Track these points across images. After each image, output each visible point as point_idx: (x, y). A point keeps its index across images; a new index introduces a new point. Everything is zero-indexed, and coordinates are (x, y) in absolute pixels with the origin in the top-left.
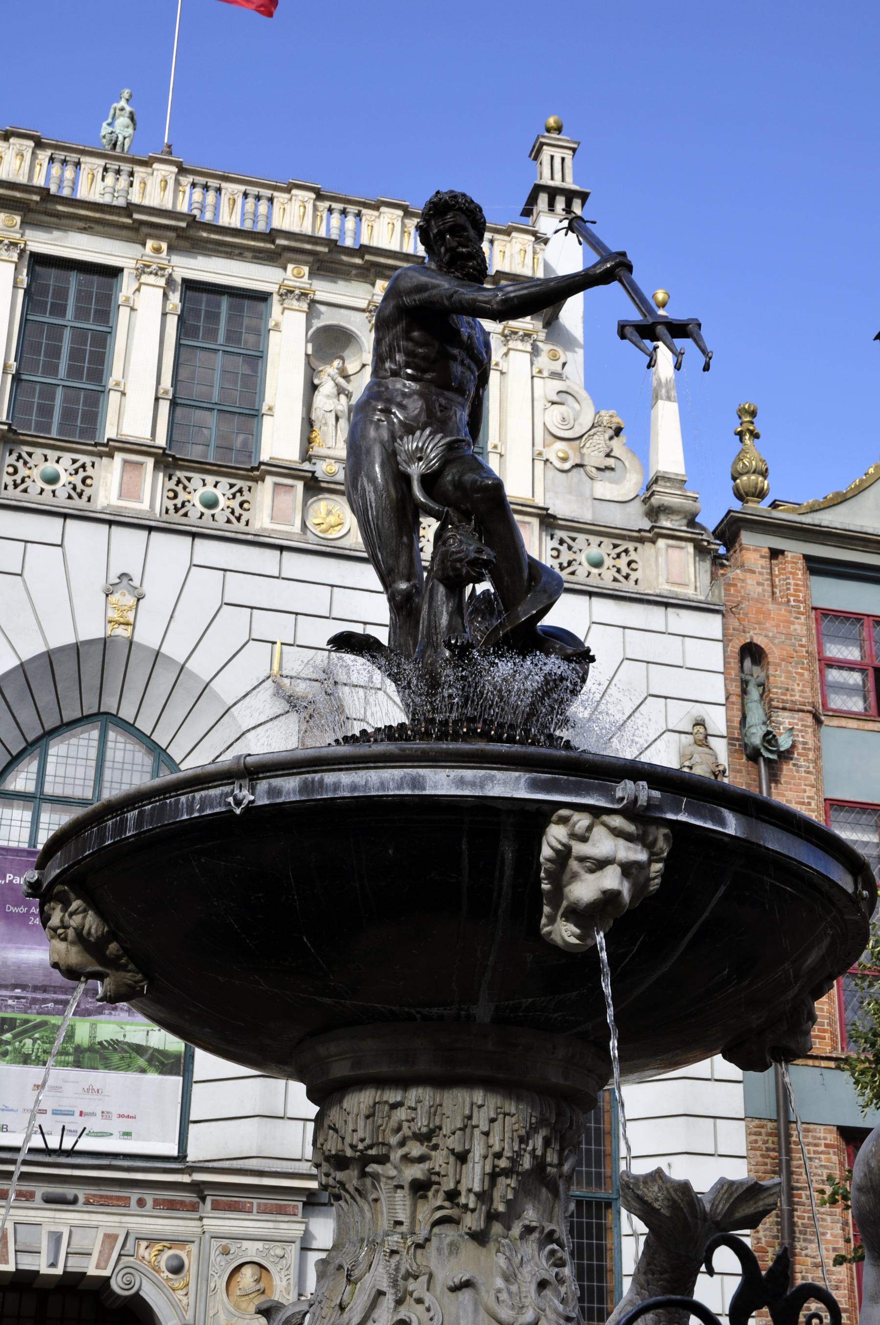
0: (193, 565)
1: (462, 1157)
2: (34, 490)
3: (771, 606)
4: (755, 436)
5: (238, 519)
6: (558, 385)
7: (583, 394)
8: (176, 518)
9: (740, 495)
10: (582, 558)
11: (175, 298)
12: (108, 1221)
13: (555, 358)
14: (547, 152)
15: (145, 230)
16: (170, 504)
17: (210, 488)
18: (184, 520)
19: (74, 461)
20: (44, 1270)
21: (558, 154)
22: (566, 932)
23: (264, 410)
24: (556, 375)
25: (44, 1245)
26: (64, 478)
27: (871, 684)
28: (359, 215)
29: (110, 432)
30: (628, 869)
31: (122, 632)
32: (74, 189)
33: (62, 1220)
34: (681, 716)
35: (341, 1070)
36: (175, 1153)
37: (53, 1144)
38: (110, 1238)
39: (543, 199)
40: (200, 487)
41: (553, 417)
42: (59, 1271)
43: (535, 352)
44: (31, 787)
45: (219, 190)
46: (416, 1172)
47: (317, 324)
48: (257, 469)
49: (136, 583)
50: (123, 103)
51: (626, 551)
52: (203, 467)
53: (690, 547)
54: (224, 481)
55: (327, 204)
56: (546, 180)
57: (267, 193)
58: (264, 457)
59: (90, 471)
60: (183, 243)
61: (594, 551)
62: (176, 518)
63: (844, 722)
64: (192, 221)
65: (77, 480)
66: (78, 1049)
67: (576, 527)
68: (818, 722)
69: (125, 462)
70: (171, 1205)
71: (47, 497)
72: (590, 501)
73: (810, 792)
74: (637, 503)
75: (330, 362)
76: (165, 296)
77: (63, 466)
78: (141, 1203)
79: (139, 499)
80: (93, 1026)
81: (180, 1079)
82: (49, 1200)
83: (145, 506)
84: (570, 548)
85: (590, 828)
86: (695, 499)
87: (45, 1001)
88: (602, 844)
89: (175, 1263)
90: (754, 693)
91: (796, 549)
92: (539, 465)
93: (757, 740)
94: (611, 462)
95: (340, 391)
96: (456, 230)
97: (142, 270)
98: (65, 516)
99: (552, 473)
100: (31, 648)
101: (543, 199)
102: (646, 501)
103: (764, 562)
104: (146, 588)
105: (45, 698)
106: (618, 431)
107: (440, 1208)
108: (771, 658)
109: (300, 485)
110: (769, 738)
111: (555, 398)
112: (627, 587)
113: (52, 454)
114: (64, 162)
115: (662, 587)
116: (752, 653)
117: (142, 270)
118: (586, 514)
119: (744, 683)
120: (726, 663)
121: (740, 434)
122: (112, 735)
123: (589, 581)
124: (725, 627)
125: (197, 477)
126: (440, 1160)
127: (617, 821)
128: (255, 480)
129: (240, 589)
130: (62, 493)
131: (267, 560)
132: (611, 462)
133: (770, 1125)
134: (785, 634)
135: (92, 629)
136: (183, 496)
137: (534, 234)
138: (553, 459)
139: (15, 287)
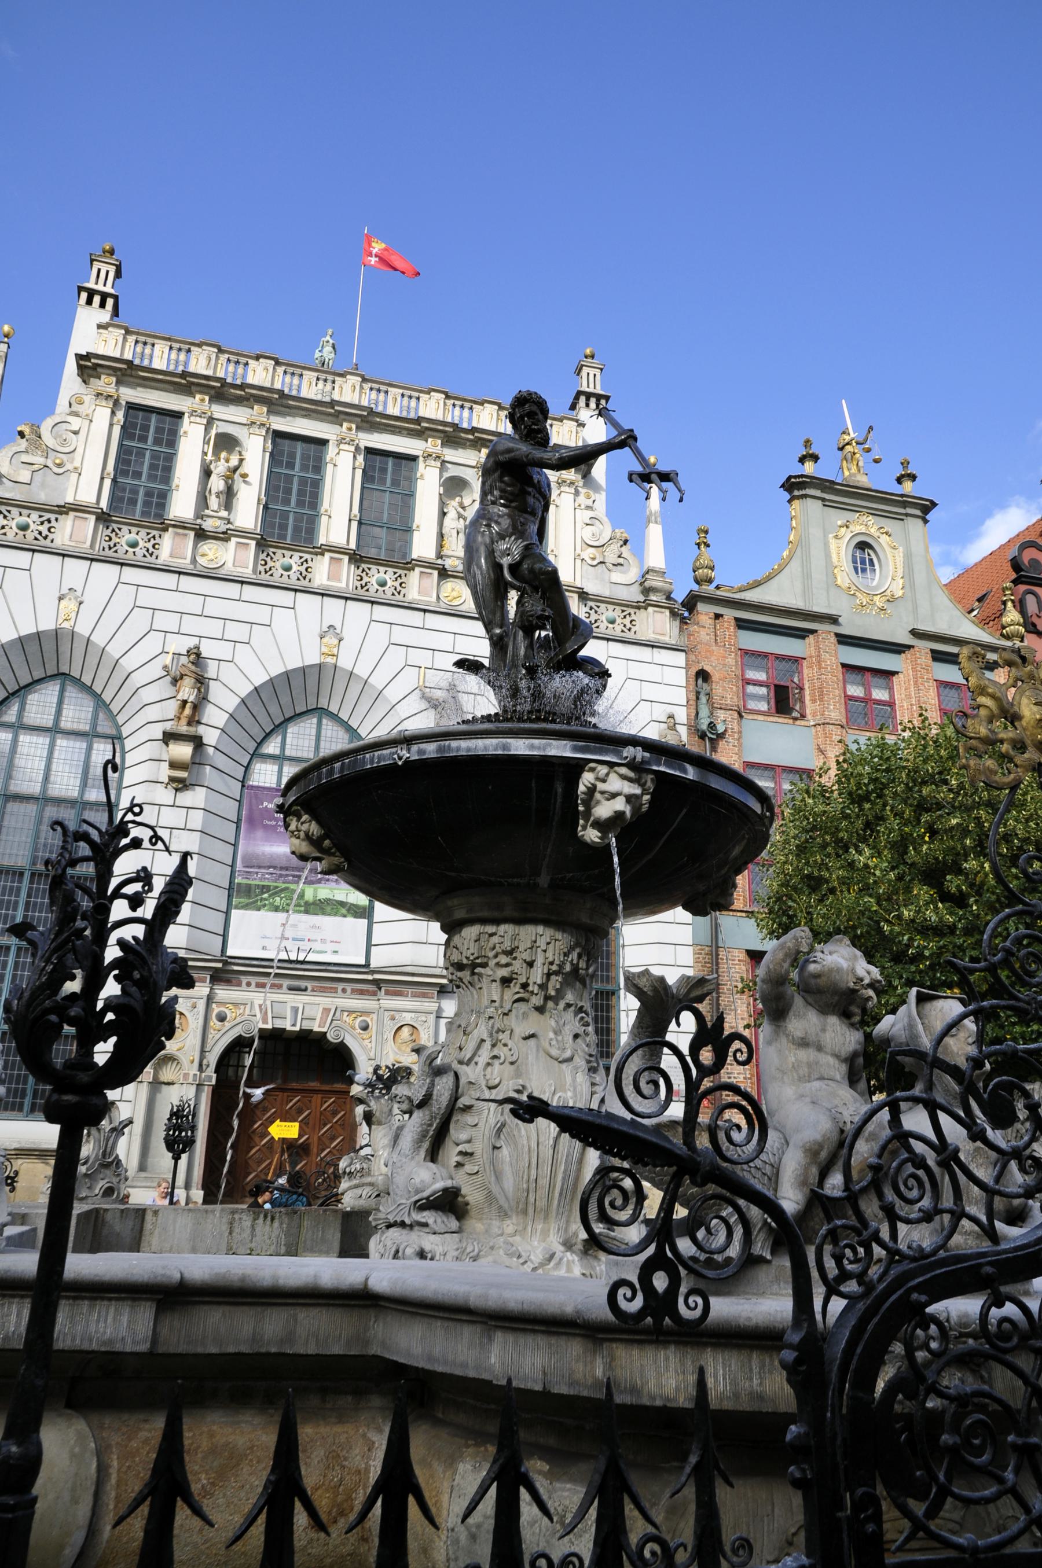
0: (372, 620)
1: (530, 964)
2: (277, 575)
3: (714, 648)
4: (707, 545)
5: (399, 593)
6: (591, 514)
7: (605, 519)
8: (362, 592)
9: (697, 581)
10: (603, 618)
11: (360, 459)
12: (325, 1001)
13: (588, 497)
14: (585, 370)
15: (342, 417)
16: (358, 584)
17: (382, 574)
18: (366, 594)
19: (301, 558)
20: (289, 1028)
21: (592, 371)
22: (592, 835)
23: (414, 527)
25: (289, 1014)
26: (295, 568)
27: (772, 694)
28: (471, 408)
29: (322, 540)
30: (629, 798)
31: (330, 660)
32: (299, 391)
33: (299, 1000)
34: (660, 712)
35: (460, 914)
36: (363, 962)
37: (293, 957)
38: (326, 1011)
39: (583, 399)
40: (376, 574)
41: (587, 533)
42: (297, 1028)
43: (577, 493)
44: (277, 752)
45: (386, 392)
46: (504, 972)
47: (446, 475)
48: (410, 563)
49: (338, 631)
50: (328, 338)
51: (630, 614)
52: (377, 562)
53: (667, 612)
54: (391, 570)
55: (452, 401)
56: (584, 388)
57: (416, 394)
58: (414, 556)
59: (310, 564)
60: (364, 425)
61: (610, 614)
62: (362, 592)
63: (755, 717)
64: (371, 412)
65: (303, 569)
66: (307, 903)
67: (600, 600)
68: (741, 716)
69: (331, 558)
70: (361, 992)
71: (285, 579)
72: (608, 584)
73: (735, 757)
74: (637, 585)
75: (454, 499)
76: (355, 457)
77: (294, 560)
78: (344, 991)
79: (340, 581)
80: (315, 890)
81: (366, 921)
82: (290, 989)
83: (343, 585)
84: (596, 612)
85: (607, 775)
86: (671, 584)
87: (287, 875)
88: (615, 783)
89: (364, 1025)
90: (703, 699)
91: (730, 614)
92: (578, 562)
93: (704, 727)
94: (621, 561)
95: (460, 516)
96: (531, 415)
97: (341, 441)
98: (296, 591)
99: (586, 567)
100: (277, 669)
101: (583, 399)
102: (641, 584)
103: (711, 621)
104: (344, 635)
105: (285, 699)
106: (626, 542)
107: (518, 993)
109: (436, 573)
110: (712, 726)
111: (589, 522)
112: (629, 636)
113: (288, 553)
114: (293, 374)
115: (650, 636)
116: (703, 675)
117: (341, 441)
118: (605, 592)
119: (698, 693)
121: (698, 544)
122: (324, 721)
123: (607, 632)
125: (374, 568)
126: (518, 966)
127: (623, 770)
128: (409, 570)
129: (400, 635)
130: (294, 577)
131: (416, 618)
132: (621, 561)
133: (707, 949)
134: (722, 664)
135: (312, 658)
136: (366, 579)
137: (577, 421)
138: (587, 558)
139: (264, 451)
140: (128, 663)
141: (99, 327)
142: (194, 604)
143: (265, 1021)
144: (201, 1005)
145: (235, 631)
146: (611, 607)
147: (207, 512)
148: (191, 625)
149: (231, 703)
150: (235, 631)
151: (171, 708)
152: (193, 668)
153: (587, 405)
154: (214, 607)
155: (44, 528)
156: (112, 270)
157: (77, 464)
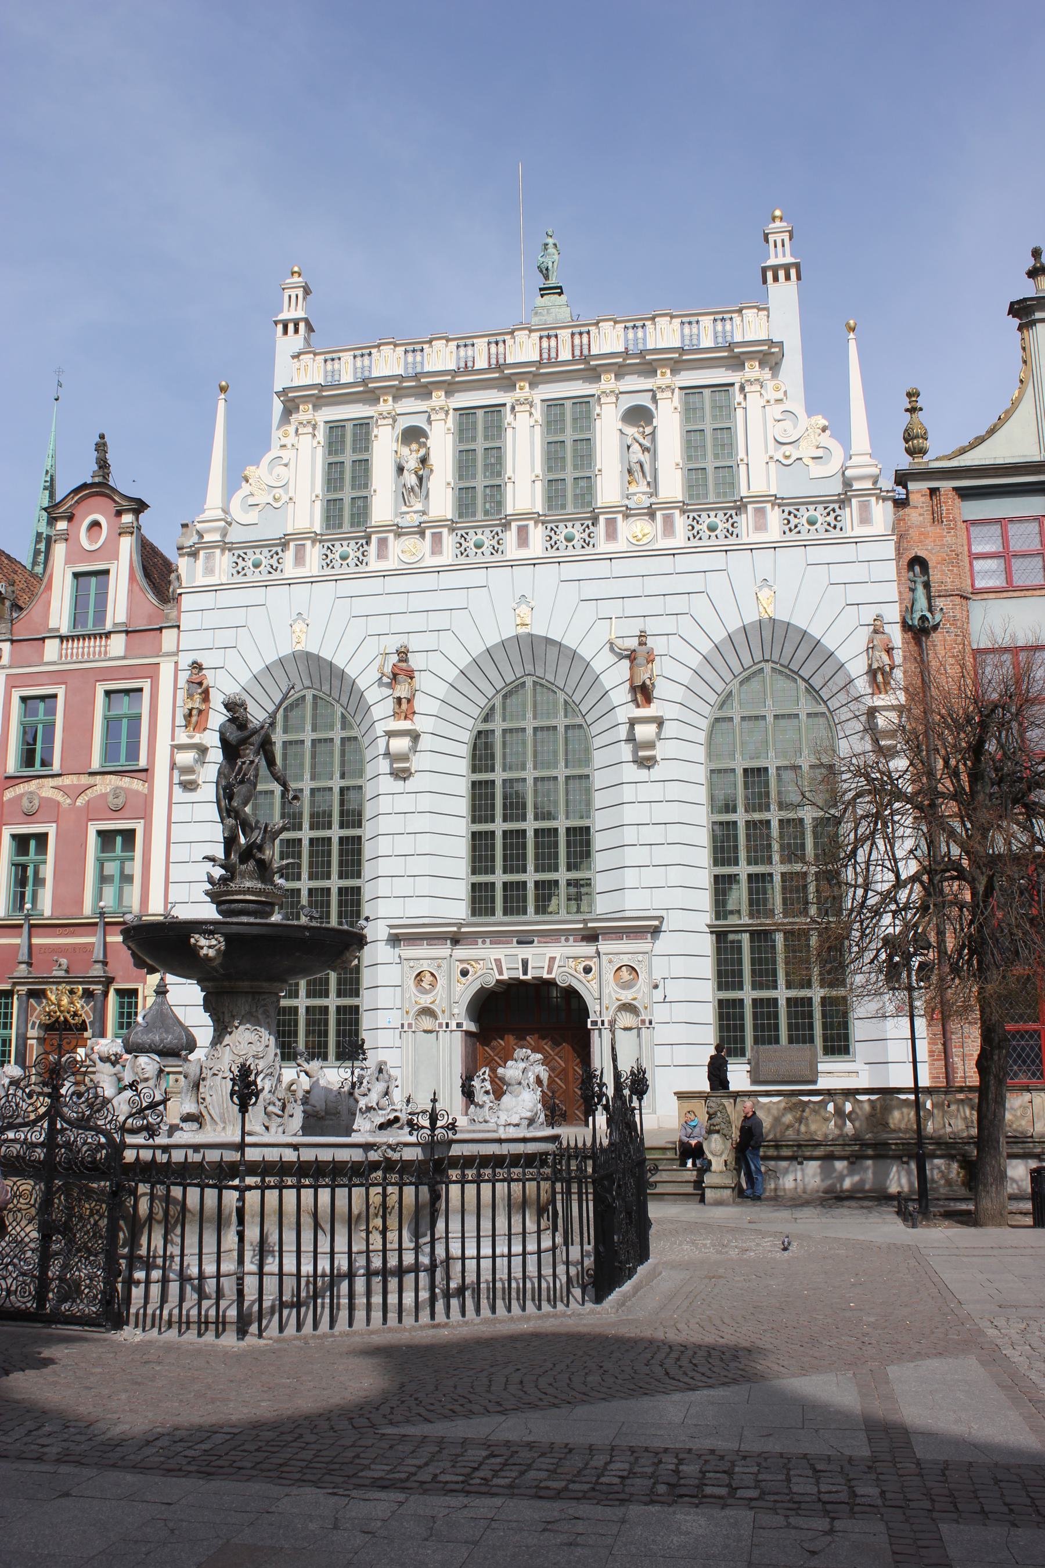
9: (910, 452)
13: (777, 389)
20: (522, 977)
21: (779, 238)
24: (779, 401)
34: (868, 615)
38: (552, 959)
39: (770, 275)
42: (529, 977)
51: (834, 510)
63: (986, 596)
82: (519, 942)
91: (946, 485)
92: (772, 465)
94: (819, 453)
106: (824, 430)
108: (930, 565)
116: (918, 563)
120: (899, 573)
124: (898, 549)
129: (591, 590)
140: (351, 671)
141: (293, 357)
142: (398, 604)
143: (501, 973)
144: (444, 964)
145: (437, 621)
146: (811, 507)
147: (404, 509)
148: (401, 623)
149: (441, 690)
150: (437, 621)
151: (389, 705)
152: (403, 665)
153: (776, 279)
154: (418, 602)
155: (274, 562)
156: (300, 292)
157: (291, 494)
